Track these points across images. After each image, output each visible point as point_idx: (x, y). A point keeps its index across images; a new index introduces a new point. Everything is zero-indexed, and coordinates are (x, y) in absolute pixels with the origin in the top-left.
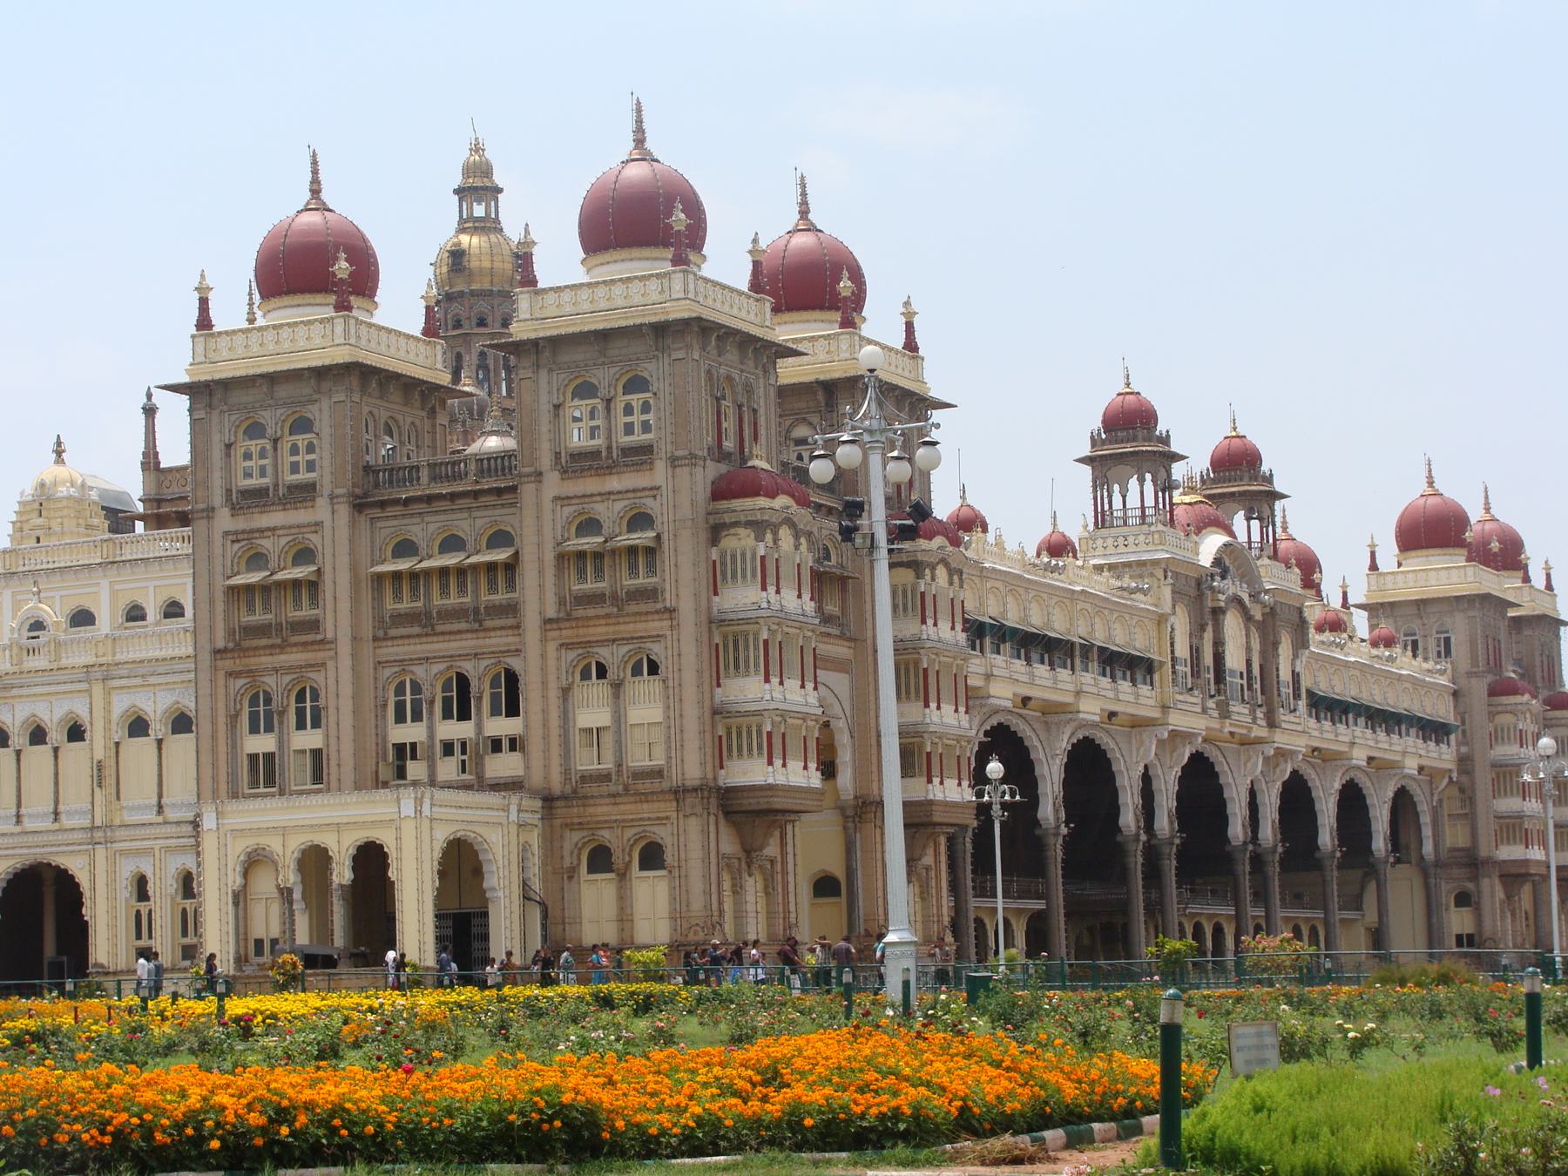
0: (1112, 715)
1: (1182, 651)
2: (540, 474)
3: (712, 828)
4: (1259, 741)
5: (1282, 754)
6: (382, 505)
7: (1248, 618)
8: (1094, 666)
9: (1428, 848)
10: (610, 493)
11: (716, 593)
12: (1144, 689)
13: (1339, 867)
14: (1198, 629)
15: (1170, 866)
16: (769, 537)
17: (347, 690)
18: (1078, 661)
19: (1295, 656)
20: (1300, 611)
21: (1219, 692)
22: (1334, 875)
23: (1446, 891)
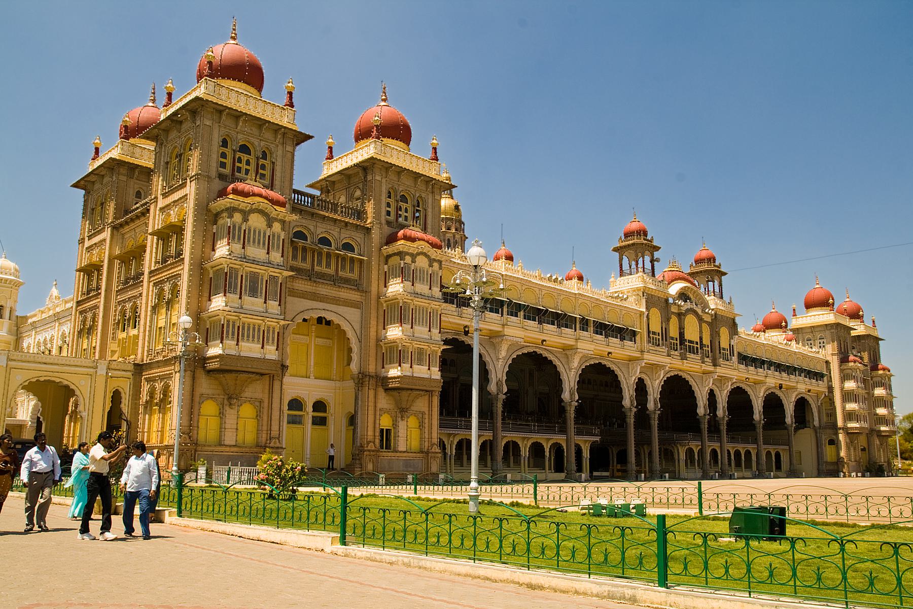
0: (609, 353)
1: (656, 327)
2: (156, 198)
3: (188, 380)
4: (711, 372)
5: (722, 380)
6: (122, 225)
7: (700, 320)
8: (591, 329)
9: (816, 423)
10: (174, 202)
11: (214, 250)
12: (628, 343)
13: (766, 427)
14: (666, 319)
15: (655, 423)
16: (238, 217)
17: (101, 315)
18: (578, 326)
19: (731, 338)
20: (734, 320)
21: (681, 349)
22: (760, 430)
23: (825, 439)
